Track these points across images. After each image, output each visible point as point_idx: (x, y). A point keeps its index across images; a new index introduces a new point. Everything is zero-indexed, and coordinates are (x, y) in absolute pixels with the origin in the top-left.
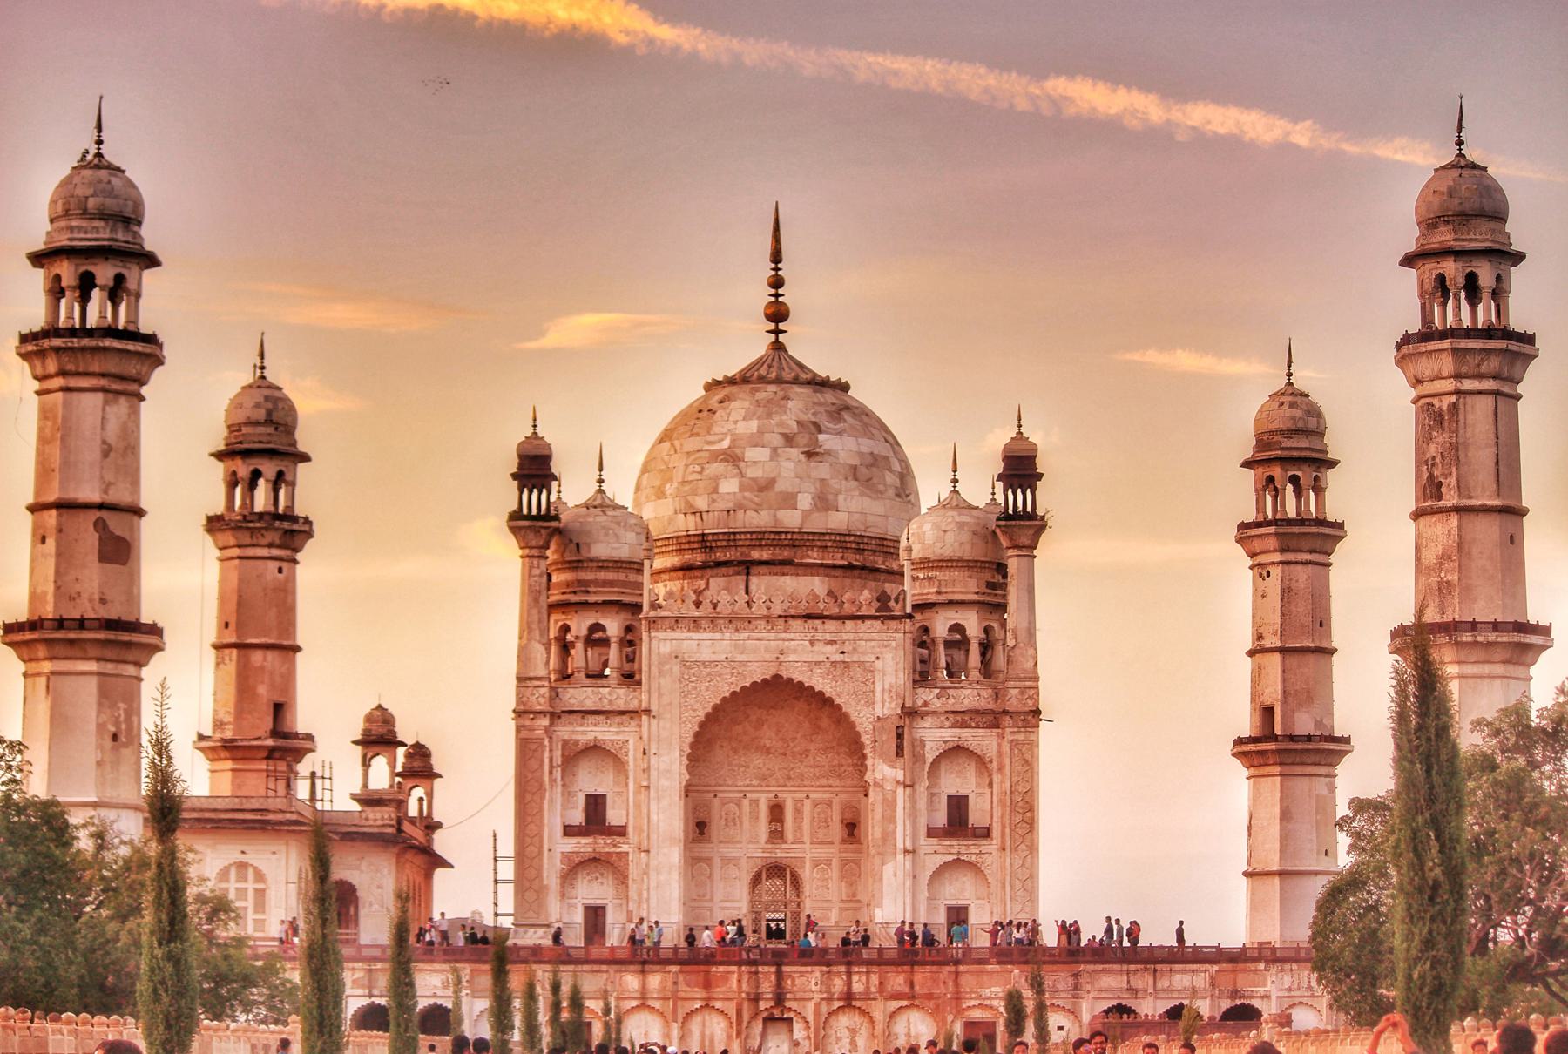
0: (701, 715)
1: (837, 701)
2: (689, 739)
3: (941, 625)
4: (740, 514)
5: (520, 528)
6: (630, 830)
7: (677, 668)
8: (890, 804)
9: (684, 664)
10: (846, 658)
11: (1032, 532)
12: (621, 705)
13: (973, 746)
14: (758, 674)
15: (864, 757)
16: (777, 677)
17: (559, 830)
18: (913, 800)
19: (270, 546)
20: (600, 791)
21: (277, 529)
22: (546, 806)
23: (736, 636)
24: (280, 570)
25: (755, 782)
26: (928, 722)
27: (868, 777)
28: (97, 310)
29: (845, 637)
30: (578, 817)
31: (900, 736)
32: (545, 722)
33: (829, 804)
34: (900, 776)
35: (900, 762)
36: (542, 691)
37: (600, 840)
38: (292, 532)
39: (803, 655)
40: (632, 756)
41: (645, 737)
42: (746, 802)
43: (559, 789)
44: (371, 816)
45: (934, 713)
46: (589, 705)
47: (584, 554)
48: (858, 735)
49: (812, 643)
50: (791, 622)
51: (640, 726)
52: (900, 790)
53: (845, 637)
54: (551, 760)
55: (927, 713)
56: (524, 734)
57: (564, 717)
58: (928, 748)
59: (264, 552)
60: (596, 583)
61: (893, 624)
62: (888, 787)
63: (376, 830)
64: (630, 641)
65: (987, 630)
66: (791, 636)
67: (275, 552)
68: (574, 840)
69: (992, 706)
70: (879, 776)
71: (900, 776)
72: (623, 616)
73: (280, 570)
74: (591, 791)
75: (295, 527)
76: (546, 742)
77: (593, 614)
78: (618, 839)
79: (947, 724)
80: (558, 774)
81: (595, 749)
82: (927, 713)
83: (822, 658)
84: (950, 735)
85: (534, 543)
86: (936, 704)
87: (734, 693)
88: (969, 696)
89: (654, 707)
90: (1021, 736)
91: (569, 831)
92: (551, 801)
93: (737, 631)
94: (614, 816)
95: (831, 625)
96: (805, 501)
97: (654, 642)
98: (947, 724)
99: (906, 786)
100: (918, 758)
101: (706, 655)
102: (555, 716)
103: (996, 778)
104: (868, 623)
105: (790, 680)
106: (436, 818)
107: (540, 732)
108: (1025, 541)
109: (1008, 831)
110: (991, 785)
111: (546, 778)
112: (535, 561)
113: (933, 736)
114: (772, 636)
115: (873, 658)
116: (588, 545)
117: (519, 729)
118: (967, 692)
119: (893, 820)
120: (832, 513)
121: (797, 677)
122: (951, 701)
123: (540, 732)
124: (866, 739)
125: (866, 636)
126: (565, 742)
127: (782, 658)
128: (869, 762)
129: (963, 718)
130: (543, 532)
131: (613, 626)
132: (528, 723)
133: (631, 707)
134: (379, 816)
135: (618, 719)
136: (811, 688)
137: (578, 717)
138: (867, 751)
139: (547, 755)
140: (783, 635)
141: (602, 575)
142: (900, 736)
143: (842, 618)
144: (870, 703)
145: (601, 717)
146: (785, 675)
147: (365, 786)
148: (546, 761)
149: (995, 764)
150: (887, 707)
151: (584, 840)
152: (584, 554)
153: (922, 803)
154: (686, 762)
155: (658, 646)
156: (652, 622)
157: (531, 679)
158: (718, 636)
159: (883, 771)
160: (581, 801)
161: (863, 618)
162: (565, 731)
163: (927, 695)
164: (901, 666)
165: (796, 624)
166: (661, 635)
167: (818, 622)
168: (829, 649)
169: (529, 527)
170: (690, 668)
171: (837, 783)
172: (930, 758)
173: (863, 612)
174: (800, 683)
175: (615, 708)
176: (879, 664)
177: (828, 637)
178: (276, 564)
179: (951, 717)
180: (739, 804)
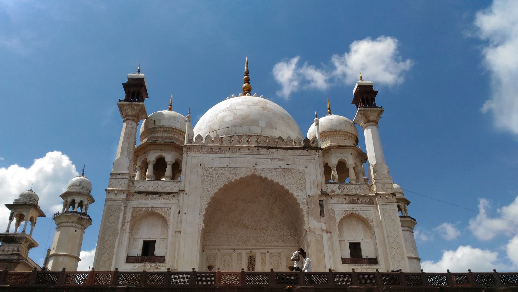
0: (212, 193)
1: (286, 187)
2: (205, 205)
3: (333, 162)
4: (234, 128)
5: (124, 105)
6: (167, 259)
7: (200, 170)
8: (320, 242)
9: (204, 168)
10: (289, 167)
11: (376, 114)
12: (168, 190)
13: (361, 214)
14: (243, 174)
15: (303, 216)
16: (254, 176)
17: (124, 258)
18: (331, 238)
19: (73, 222)
20: (152, 239)
21: (76, 216)
22: (117, 243)
23: (233, 156)
24: (76, 231)
25: (240, 244)
26: (335, 200)
27: (306, 227)
28: (71, 209)
29: (288, 157)
30: (137, 251)
31: (321, 206)
32: (124, 196)
33: (279, 256)
34: (324, 227)
35: (322, 219)
36: (124, 180)
37: (148, 265)
38: (82, 218)
39: (268, 166)
40: (172, 218)
41: (181, 205)
42: (235, 255)
43: (127, 235)
44: (6, 249)
45: (338, 195)
46: (151, 190)
47: (157, 124)
48: (299, 204)
49: (272, 160)
50: (260, 149)
51: (178, 201)
52: (325, 234)
53: (288, 157)
54: (124, 219)
55: (335, 196)
56: (109, 203)
57: (136, 196)
58: (336, 213)
59: (71, 224)
60: (162, 137)
61: (313, 152)
62: (318, 232)
63: (7, 257)
64: (177, 168)
65: (355, 164)
66: (261, 156)
67: (74, 225)
68: (132, 265)
69: (368, 193)
70: (312, 227)
71: (324, 227)
72: (174, 153)
73: (76, 231)
74: (147, 238)
75: (83, 217)
76: (123, 207)
77: (160, 151)
78: (159, 264)
79: (346, 201)
80: (127, 226)
81: (152, 214)
82: (335, 196)
83: (278, 167)
84: (349, 208)
85: (130, 113)
86: (338, 192)
87: (230, 183)
88: (354, 189)
89: (187, 191)
90: (388, 207)
91: (129, 259)
92: (120, 242)
93: (233, 153)
94: (158, 251)
95: (281, 151)
96: (262, 124)
97: (189, 158)
98: (346, 201)
99: (327, 232)
100: (332, 219)
101: (216, 164)
102: (130, 195)
103: (377, 231)
104: (300, 151)
105: (261, 177)
106: (8, 212)
107: (119, 202)
108: (373, 118)
109: (389, 258)
110: (374, 234)
111: (119, 227)
112: (130, 122)
113: (339, 208)
114: (251, 156)
115: (303, 167)
116: (160, 120)
117: (107, 200)
118: (352, 187)
119: (322, 251)
120: (274, 130)
121: (264, 176)
122: (346, 190)
123: (119, 202)
124: (303, 207)
125: (299, 157)
126: (135, 209)
127: (256, 166)
128: (306, 219)
129: (355, 199)
130: (135, 107)
131: (169, 158)
132: (113, 196)
133: (176, 190)
134: (11, 248)
135: (166, 197)
136: (272, 181)
137: (143, 196)
138: (304, 213)
139: (122, 213)
140: (257, 156)
141: (165, 135)
142: (321, 206)
143: (288, 149)
144: (304, 189)
145: (157, 196)
146: (258, 174)
147: (8, 231)
148: (121, 218)
149: (374, 223)
150: (314, 191)
151: (138, 265)
152: (157, 124)
153: (337, 244)
154: (202, 218)
155: (190, 161)
156: (189, 148)
157: (119, 174)
158: (223, 156)
159: (312, 223)
160: (140, 245)
161: (297, 149)
162: (136, 202)
163: (331, 188)
164: (319, 171)
165: (264, 151)
166: (193, 155)
167: (274, 151)
168: (281, 163)
169: (129, 104)
170: (207, 170)
171: (283, 244)
172: (338, 219)
173: (298, 146)
174: (266, 179)
175: (164, 191)
176: (307, 170)
177: (280, 157)
178: (75, 229)
179: (347, 198)
180: (231, 256)
